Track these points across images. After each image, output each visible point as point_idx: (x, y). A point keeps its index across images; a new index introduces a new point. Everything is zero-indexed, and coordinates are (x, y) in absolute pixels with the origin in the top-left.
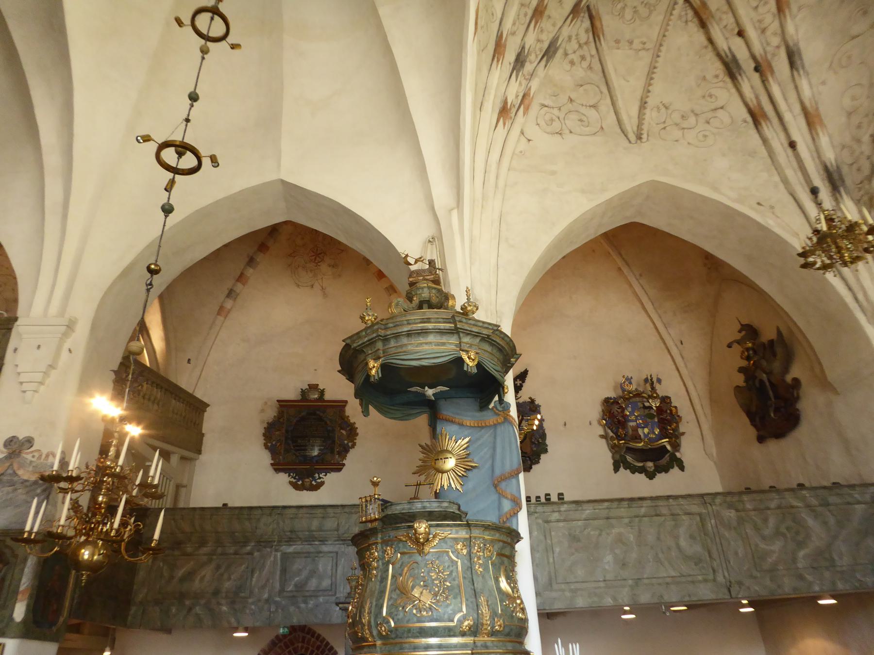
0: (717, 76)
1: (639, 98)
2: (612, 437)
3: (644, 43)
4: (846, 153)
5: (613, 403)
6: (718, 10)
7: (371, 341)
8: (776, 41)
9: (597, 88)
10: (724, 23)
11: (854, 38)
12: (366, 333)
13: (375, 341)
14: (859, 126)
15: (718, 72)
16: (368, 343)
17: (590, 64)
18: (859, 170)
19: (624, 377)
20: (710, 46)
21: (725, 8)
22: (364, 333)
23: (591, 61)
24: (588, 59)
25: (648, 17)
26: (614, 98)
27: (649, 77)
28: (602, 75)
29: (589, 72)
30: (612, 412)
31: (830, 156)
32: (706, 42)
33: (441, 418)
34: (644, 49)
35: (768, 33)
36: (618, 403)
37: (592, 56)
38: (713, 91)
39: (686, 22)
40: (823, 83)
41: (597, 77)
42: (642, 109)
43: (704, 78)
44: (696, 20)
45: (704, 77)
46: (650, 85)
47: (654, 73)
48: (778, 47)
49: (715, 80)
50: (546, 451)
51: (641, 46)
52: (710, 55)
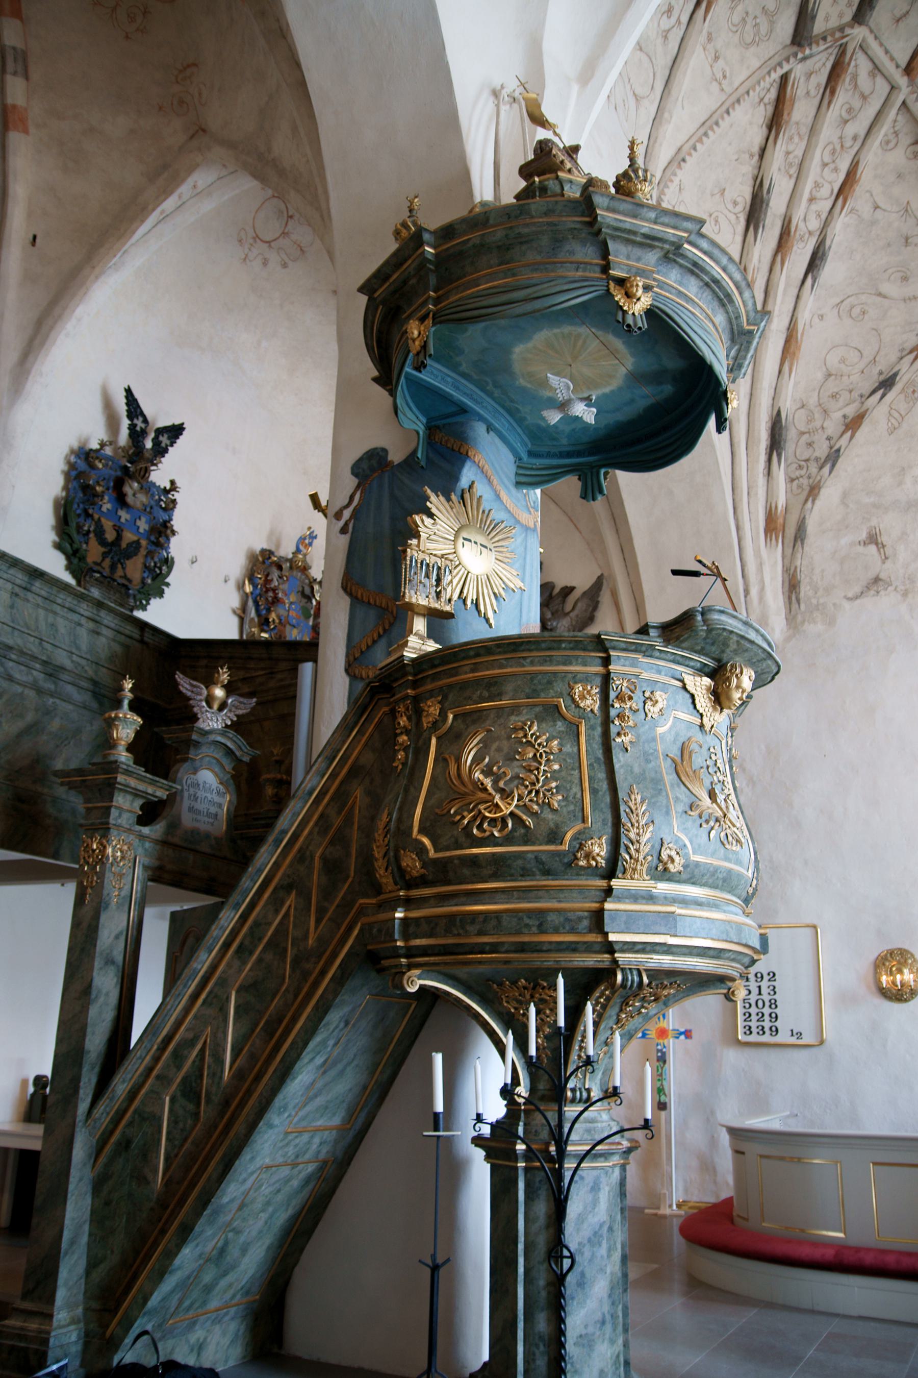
0: (735, 203)
1: (679, 144)
2: (252, 619)
3: (725, 77)
4: (801, 415)
5: (274, 563)
6: (797, 123)
7: (648, 241)
8: (814, 224)
9: (652, 75)
10: (791, 148)
11: (880, 295)
12: (656, 218)
13: (652, 247)
14: (834, 396)
15: (739, 199)
16: (638, 239)
17: (669, 30)
18: (810, 444)
19: (309, 528)
20: (756, 158)
21: (804, 130)
22: (652, 215)
23: (673, 27)
24: (673, 20)
25: (748, 46)
26: (666, 115)
27: (702, 131)
28: (670, 64)
29: (660, 40)
30: (269, 578)
31: (787, 405)
32: (756, 149)
33: (476, 460)
34: (720, 84)
35: (814, 207)
36: (280, 568)
37: (679, 21)
38: (722, 219)
39: (762, 100)
40: (821, 317)
41: (663, 61)
42: (675, 164)
43: (723, 192)
44: (770, 109)
45: (724, 190)
46: (700, 140)
47: (711, 128)
48: (810, 233)
49: (730, 206)
50: (161, 594)
51: (719, 75)
52: (748, 169)
